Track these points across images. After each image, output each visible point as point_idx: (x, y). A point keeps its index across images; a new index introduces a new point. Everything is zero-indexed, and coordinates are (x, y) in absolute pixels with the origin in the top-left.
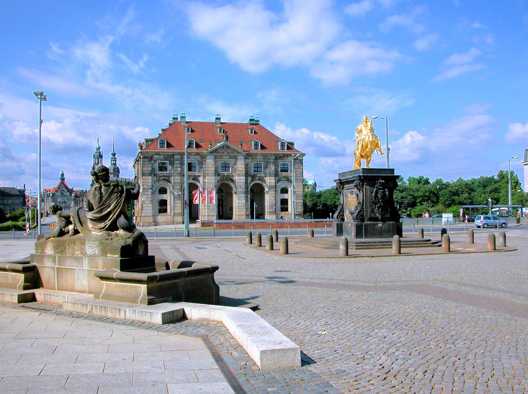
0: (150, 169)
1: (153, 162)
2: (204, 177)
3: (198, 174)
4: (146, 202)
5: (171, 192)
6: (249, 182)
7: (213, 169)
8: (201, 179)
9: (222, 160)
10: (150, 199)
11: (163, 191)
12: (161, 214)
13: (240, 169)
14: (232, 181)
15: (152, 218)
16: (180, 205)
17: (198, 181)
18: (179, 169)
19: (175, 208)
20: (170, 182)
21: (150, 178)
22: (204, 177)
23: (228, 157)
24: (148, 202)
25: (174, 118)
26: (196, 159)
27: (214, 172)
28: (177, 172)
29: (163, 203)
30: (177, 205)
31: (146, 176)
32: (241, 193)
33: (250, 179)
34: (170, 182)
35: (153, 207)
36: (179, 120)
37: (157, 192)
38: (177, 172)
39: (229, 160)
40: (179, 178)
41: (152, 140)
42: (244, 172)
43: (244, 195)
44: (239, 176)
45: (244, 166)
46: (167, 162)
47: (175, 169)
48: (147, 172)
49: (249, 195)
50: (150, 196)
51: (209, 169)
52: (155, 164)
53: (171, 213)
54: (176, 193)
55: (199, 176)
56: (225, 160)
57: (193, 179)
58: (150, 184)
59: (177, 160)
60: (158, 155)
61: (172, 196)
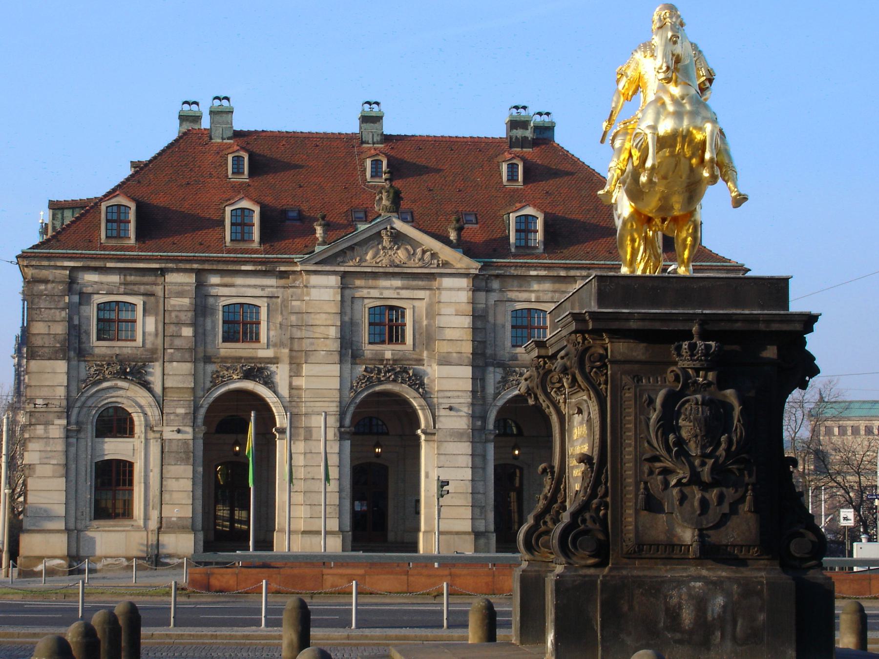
0: (60, 329)
1: (76, 299)
2: (295, 369)
3: (269, 353)
4: (39, 470)
5: (149, 427)
6: (490, 390)
7: (333, 332)
8: (281, 374)
9: (374, 293)
10: (60, 459)
11: (117, 423)
12: (101, 522)
13: (449, 334)
14: (417, 382)
15: (64, 538)
16: (188, 485)
17: (269, 383)
18: (187, 332)
19: (166, 496)
20: (146, 385)
21: (61, 366)
22: (295, 369)
23: (398, 283)
24: (48, 470)
25: (183, 118)
26: (263, 287)
27: (335, 346)
28: (178, 342)
29: (113, 479)
30: (170, 484)
31: (42, 358)
32: (457, 435)
33: (493, 376)
34: (146, 385)
35: (73, 493)
36: (206, 123)
37: (90, 429)
38: (178, 342)
39: (405, 293)
40: (187, 367)
41: (86, 209)
42: (467, 348)
43: (465, 448)
44: (444, 361)
45: (467, 321)
46: (138, 301)
47: (171, 329)
48: (48, 341)
49: (491, 448)
50: (60, 446)
51: (319, 331)
52: (85, 310)
53: (146, 518)
54: (169, 433)
55: (275, 360)
56: (387, 293)
57: (249, 375)
58: (61, 392)
59: (180, 294)
60: (96, 269)
61: (155, 449)
